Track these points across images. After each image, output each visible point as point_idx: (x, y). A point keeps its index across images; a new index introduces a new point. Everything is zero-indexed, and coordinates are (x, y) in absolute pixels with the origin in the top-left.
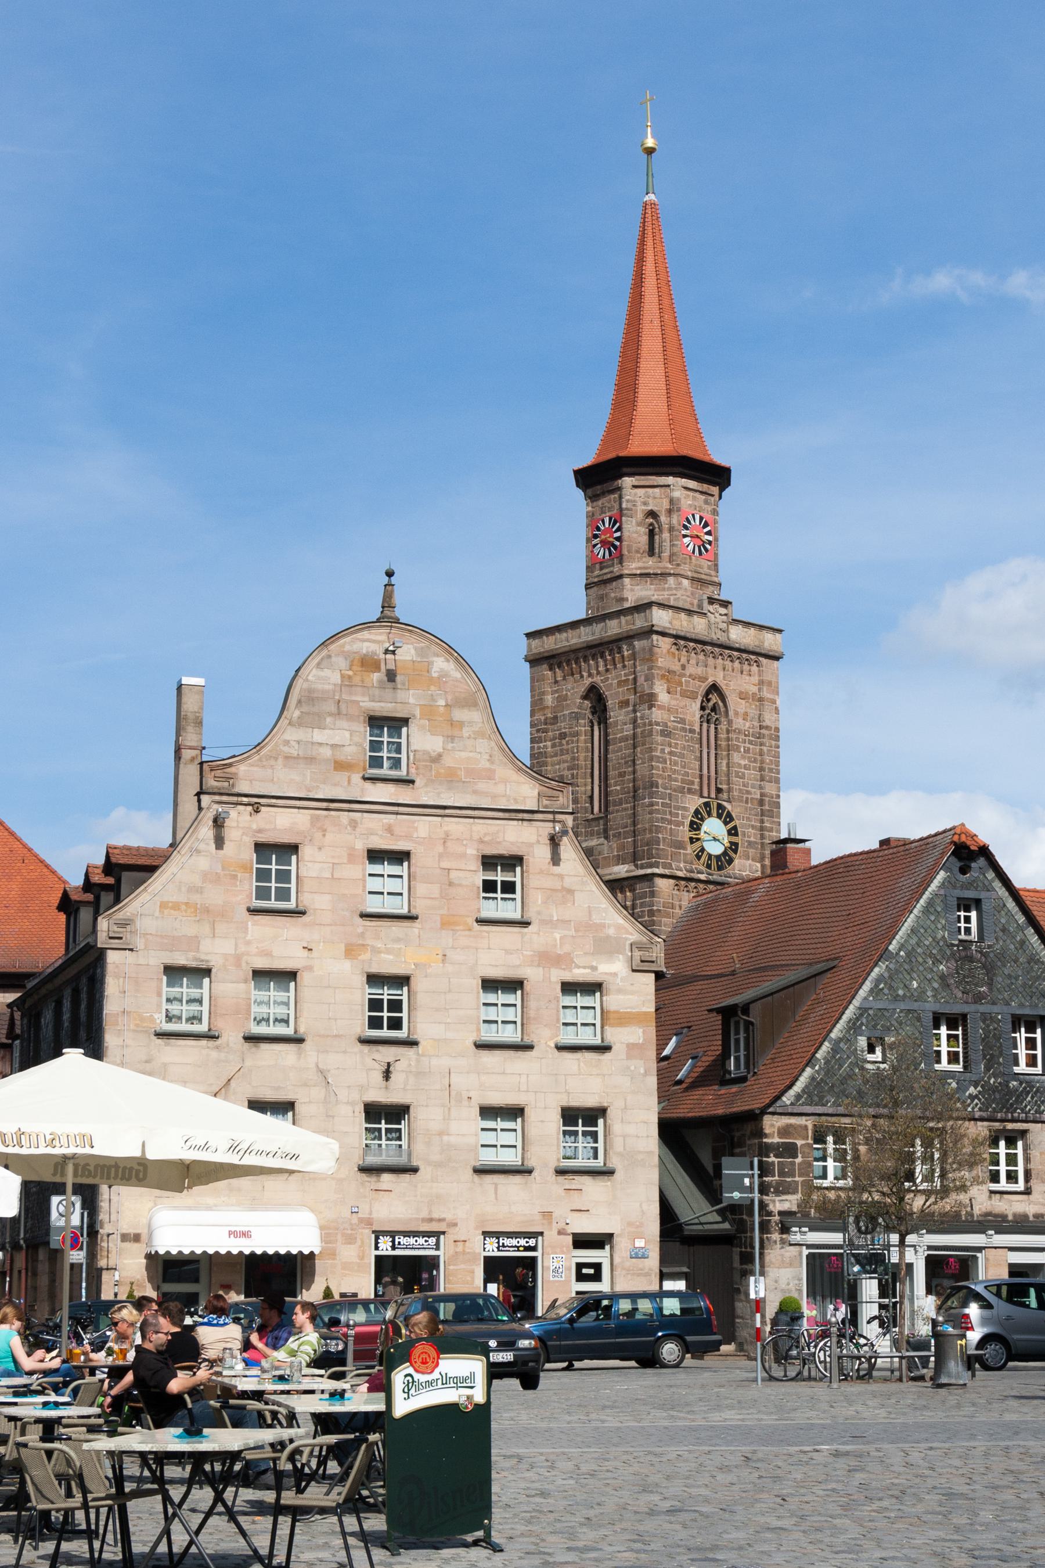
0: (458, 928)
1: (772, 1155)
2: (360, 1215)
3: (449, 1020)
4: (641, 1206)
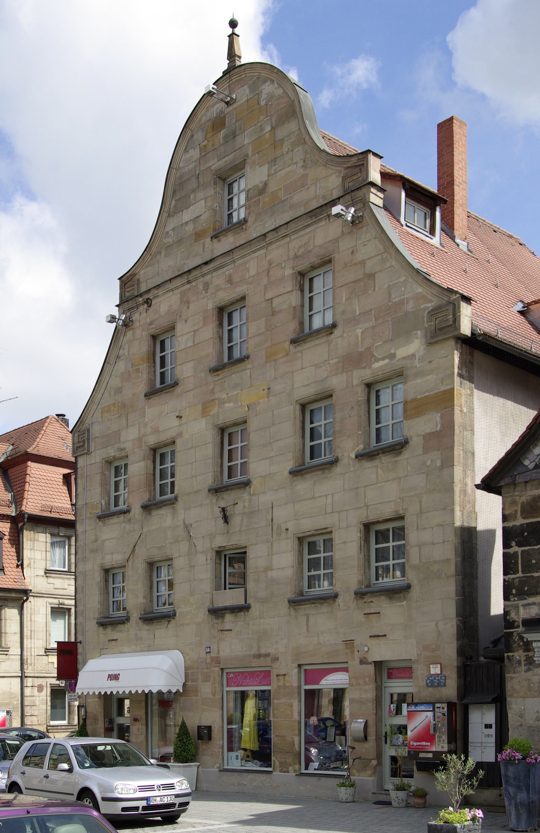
0: (279, 356)
1: (513, 544)
2: (212, 655)
3: (272, 454)
4: (437, 625)
